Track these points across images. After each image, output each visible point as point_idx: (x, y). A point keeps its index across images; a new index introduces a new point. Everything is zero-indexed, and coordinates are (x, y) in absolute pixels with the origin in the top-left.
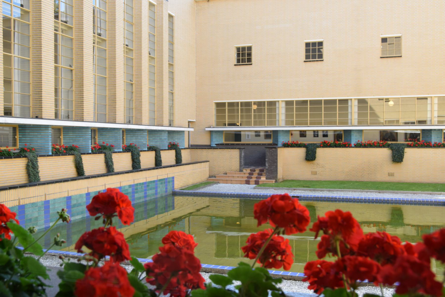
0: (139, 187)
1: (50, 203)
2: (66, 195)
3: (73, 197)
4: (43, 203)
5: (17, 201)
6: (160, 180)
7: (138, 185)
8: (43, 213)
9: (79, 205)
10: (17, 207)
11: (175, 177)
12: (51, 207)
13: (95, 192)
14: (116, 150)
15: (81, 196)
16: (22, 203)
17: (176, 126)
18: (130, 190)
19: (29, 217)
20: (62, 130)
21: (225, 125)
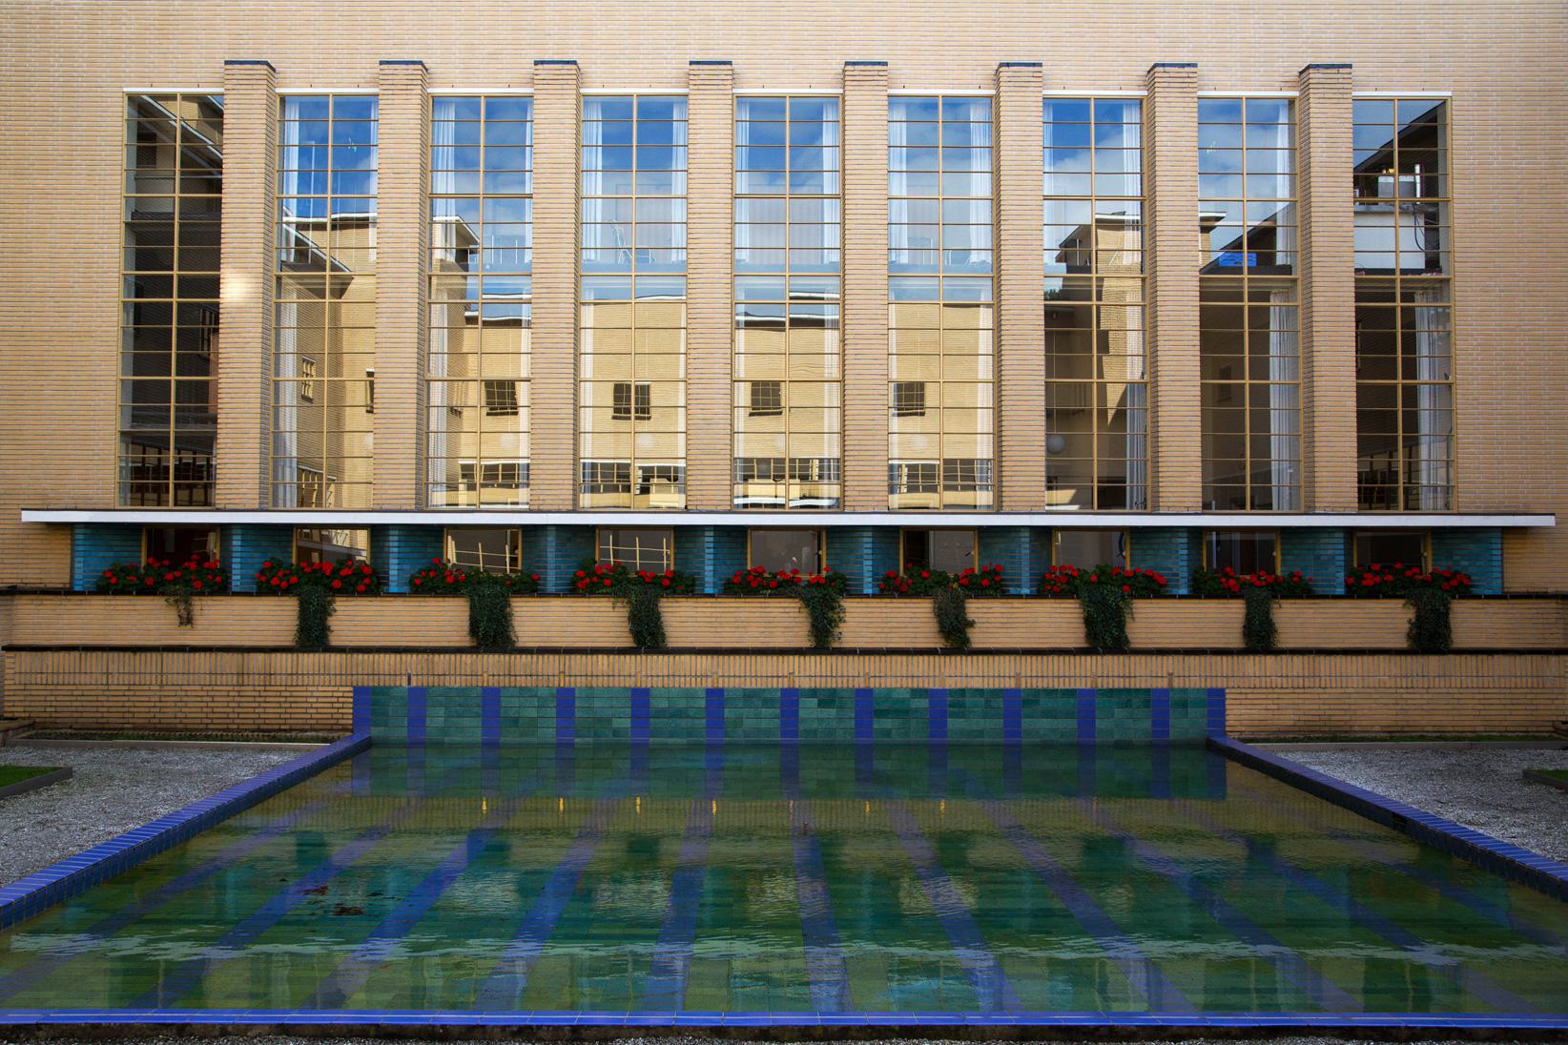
0: (968, 701)
1: (577, 692)
2: (630, 683)
3: (654, 693)
4: (555, 691)
6: (1111, 692)
7: (968, 695)
8: (552, 712)
9: (679, 714)
10: (480, 690)
11: (1227, 691)
12: (578, 704)
13: (744, 690)
14: (1012, 591)
15: (688, 694)
16: (493, 682)
17: (1462, 510)
18: (923, 703)
19: (512, 713)
20: (824, 534)
21: (1243, 507)
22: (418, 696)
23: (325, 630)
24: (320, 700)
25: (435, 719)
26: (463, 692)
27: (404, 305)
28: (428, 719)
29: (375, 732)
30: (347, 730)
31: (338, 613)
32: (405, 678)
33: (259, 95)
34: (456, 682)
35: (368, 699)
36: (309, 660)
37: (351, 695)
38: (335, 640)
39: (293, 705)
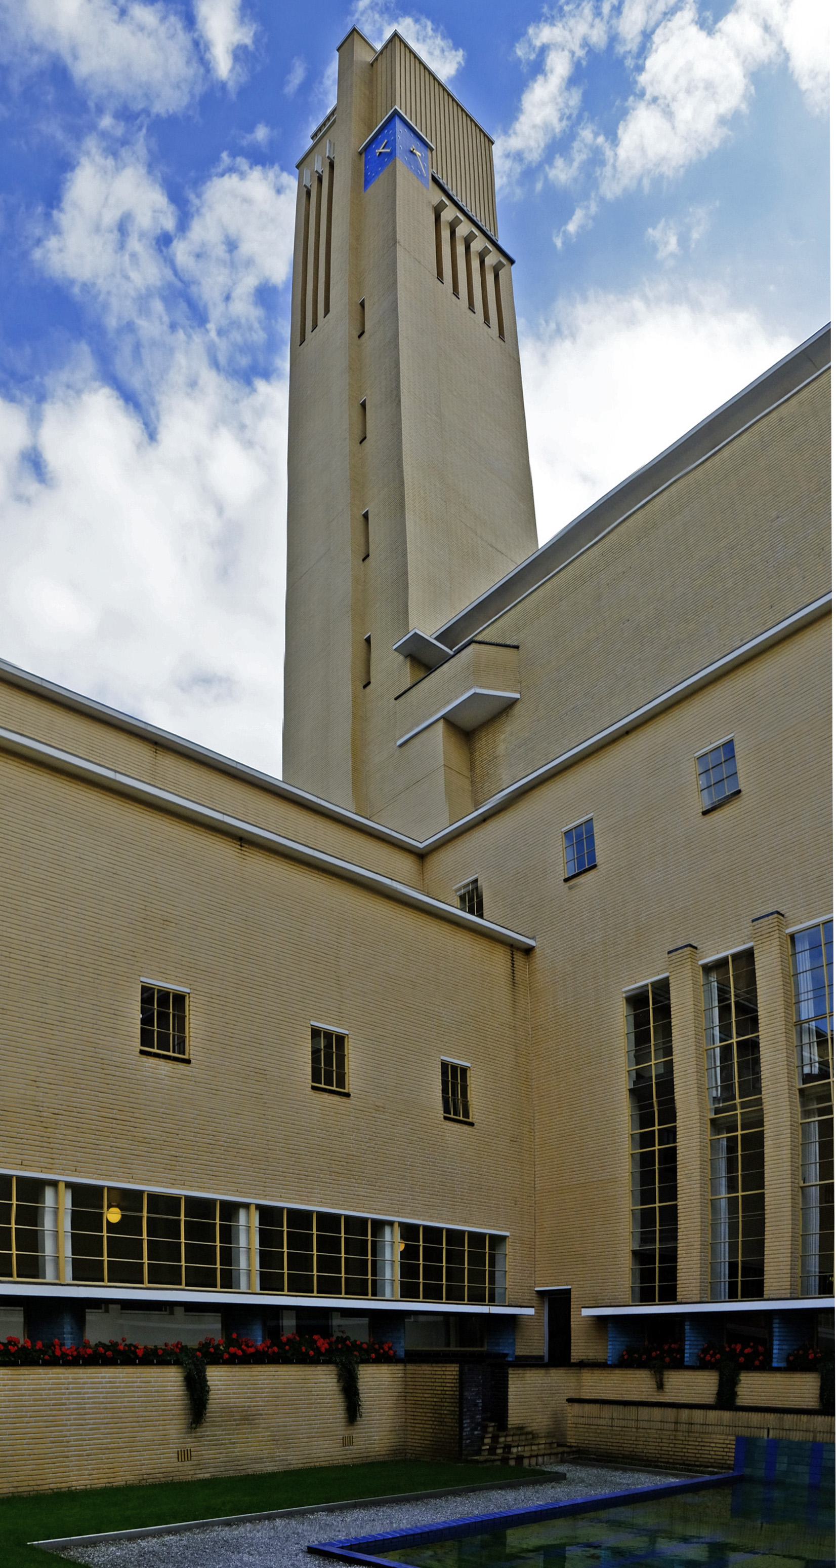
5: (812, 1434)
22: (774, 1444)
23: (734, 1395)
24: (718, 1445)
25: (782, 1465)
26: (800, 1444)
27: (781, 1128)
28: (778, 1465)
29: (747, 1471)
30: (729, 1468)
31: (742, 1382)
32: (766, 1431)
33: (687, 971)
34: (796, 1436)
35: (744, 1444)
36: (726, 1415)
37: (734, 1443)
38: (741, 1401)
39: (703, 1448)
